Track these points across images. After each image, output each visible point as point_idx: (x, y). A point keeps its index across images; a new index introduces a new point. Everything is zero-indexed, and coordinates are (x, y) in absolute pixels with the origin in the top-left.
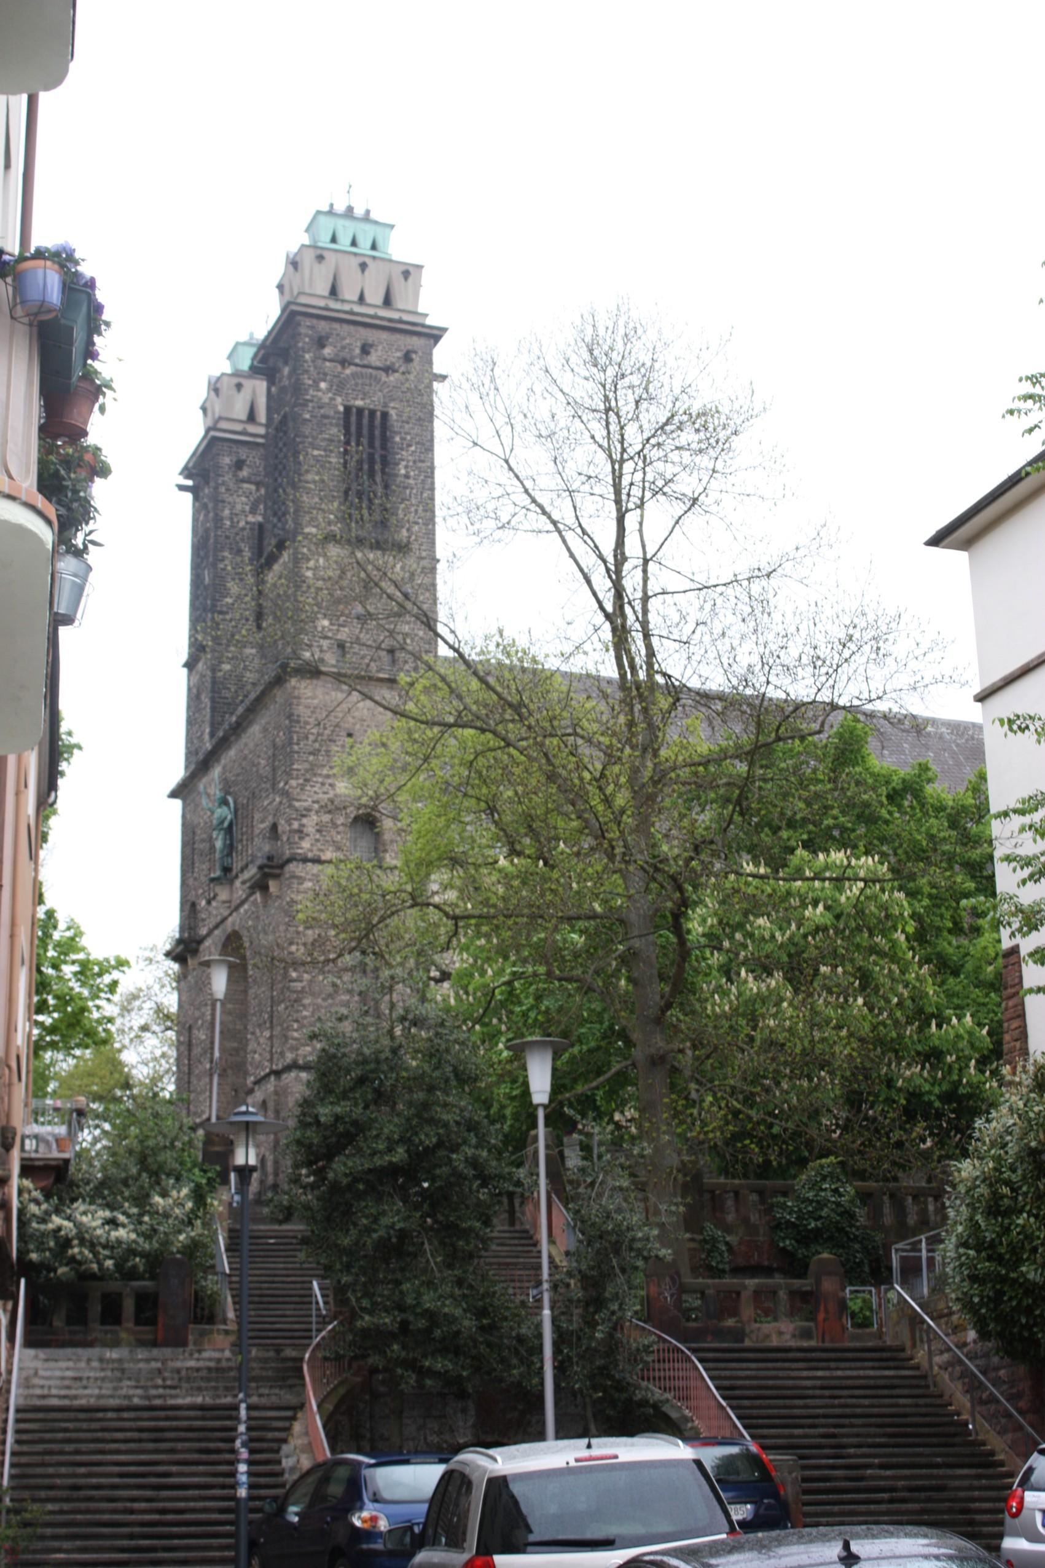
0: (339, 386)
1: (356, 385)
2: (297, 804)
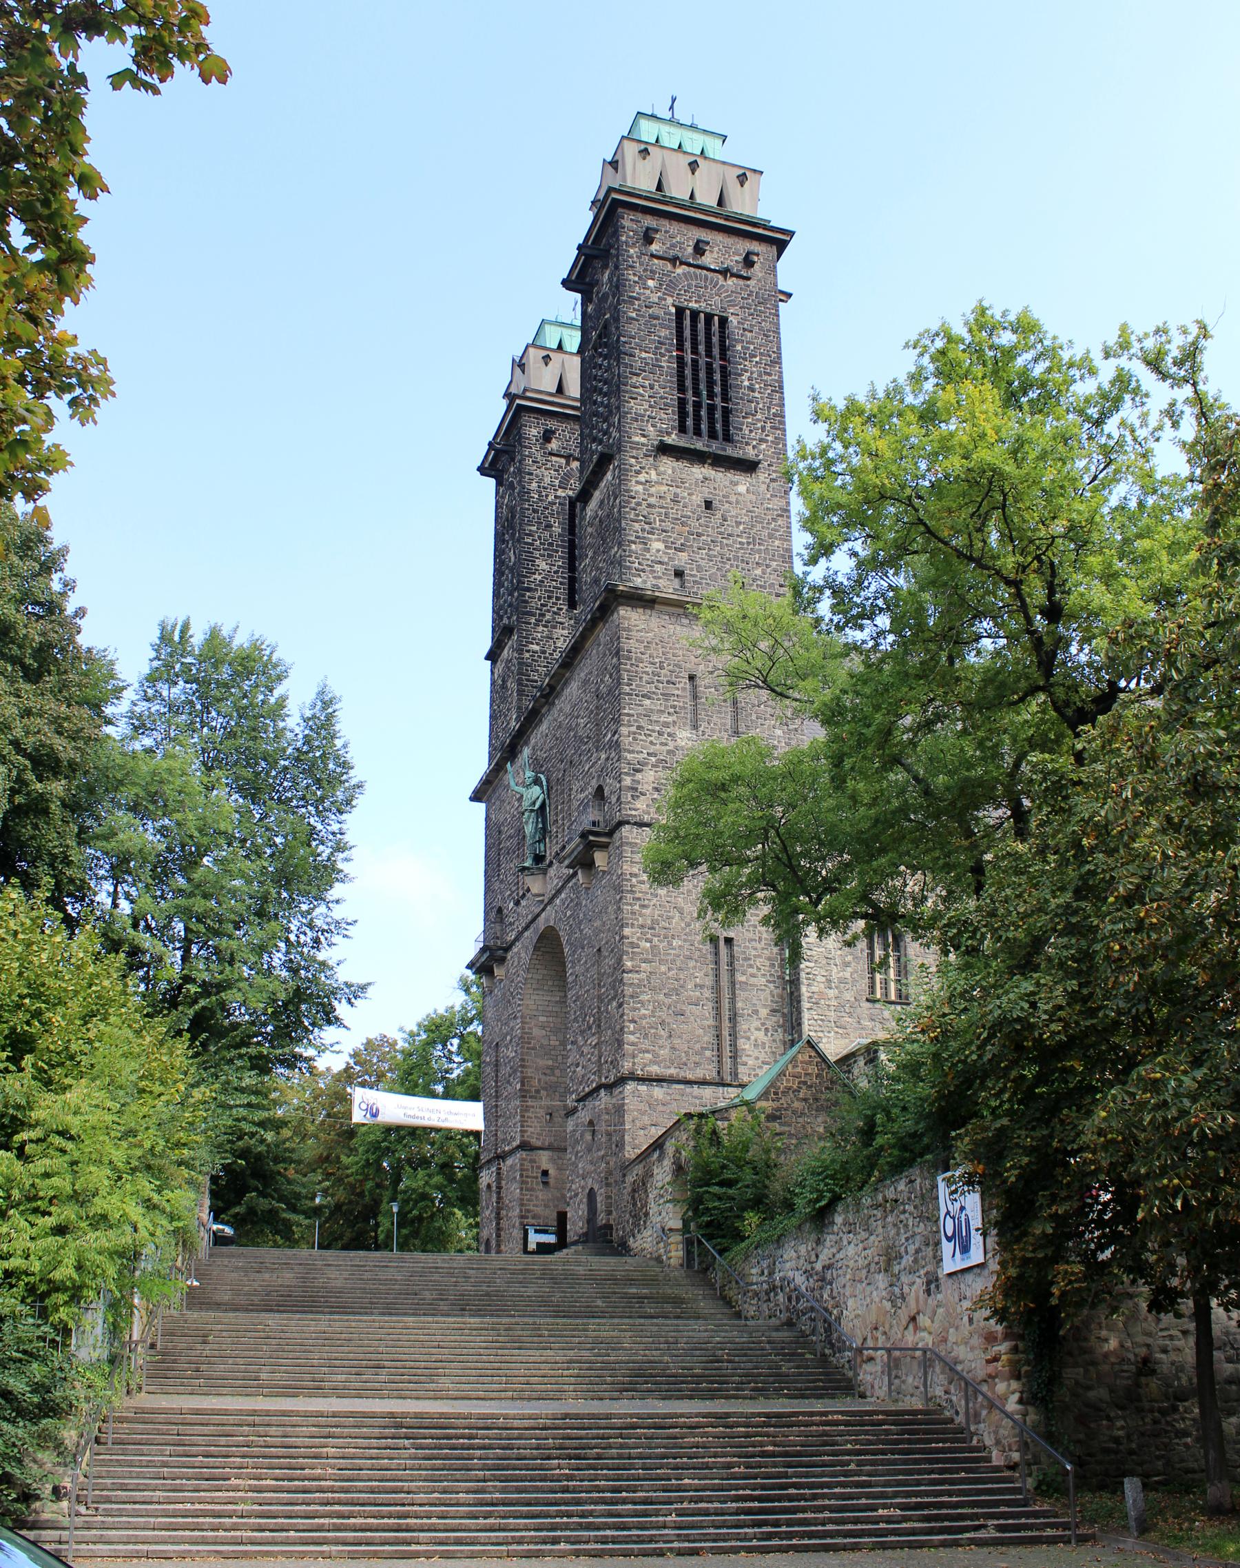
0: (670, 286)
1: (689, 286)
2: (629, 756)
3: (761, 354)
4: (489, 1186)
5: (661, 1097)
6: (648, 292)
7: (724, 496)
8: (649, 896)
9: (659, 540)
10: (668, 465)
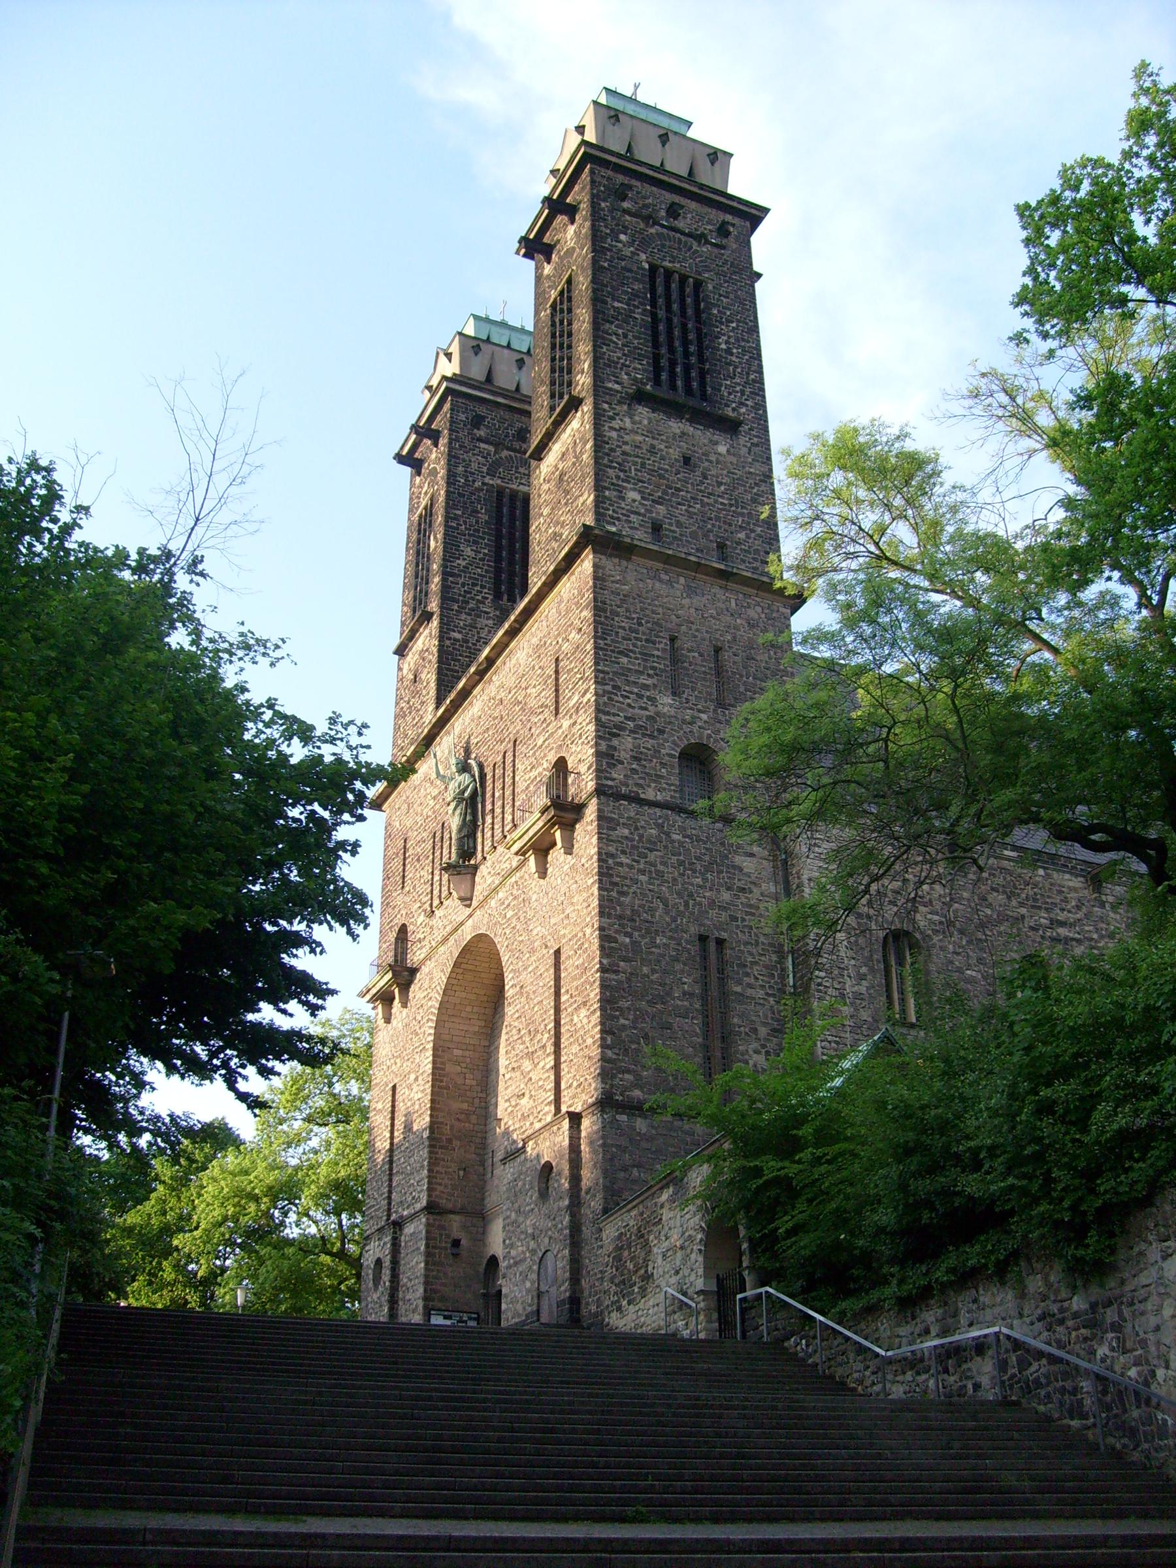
3: (738, 321)
4: (379, 1262)
5: (644, 1130)
6: (620, 245)
7: (703, 454)
8: (628, 882)
9: (634, 490)
10: (643, 413)
